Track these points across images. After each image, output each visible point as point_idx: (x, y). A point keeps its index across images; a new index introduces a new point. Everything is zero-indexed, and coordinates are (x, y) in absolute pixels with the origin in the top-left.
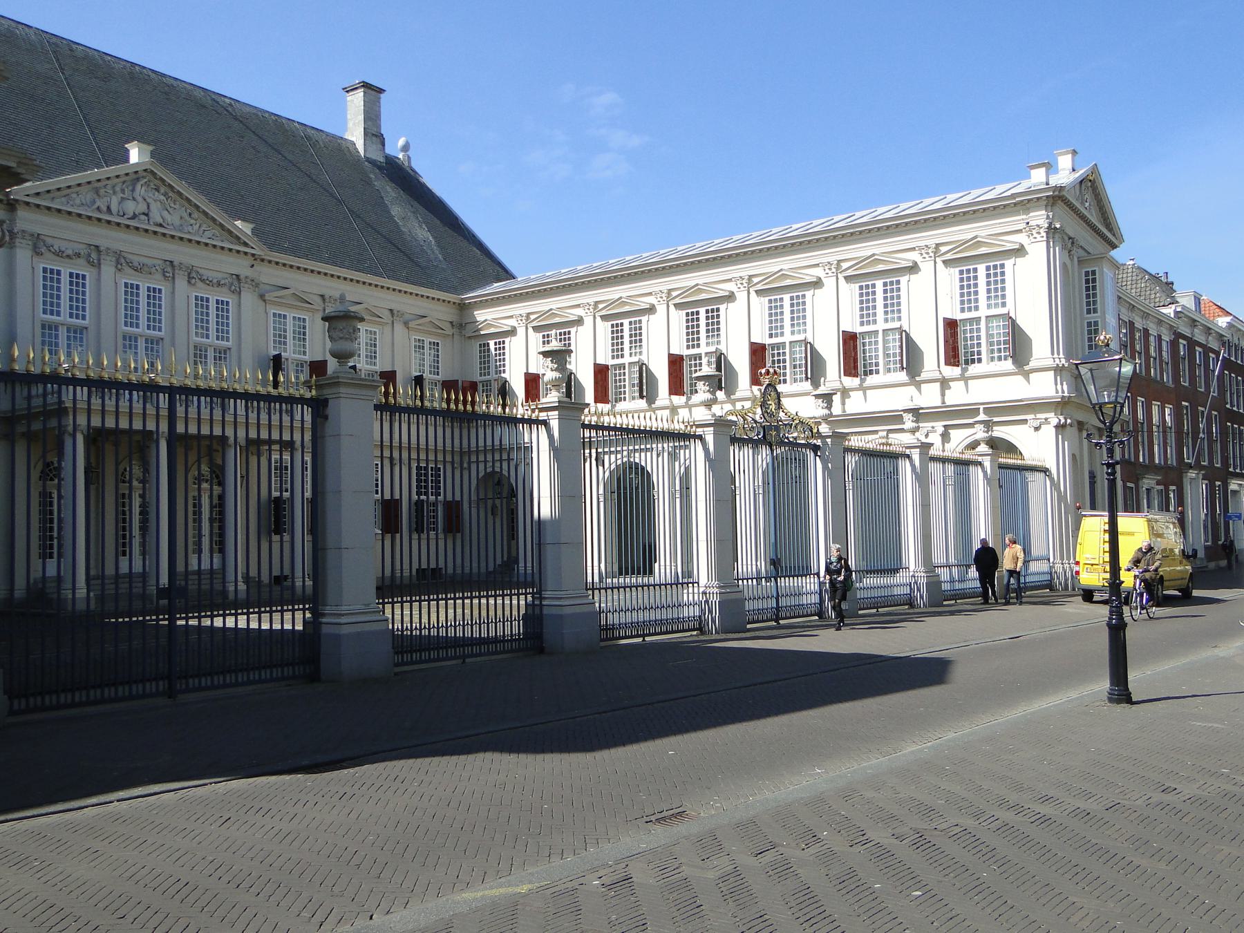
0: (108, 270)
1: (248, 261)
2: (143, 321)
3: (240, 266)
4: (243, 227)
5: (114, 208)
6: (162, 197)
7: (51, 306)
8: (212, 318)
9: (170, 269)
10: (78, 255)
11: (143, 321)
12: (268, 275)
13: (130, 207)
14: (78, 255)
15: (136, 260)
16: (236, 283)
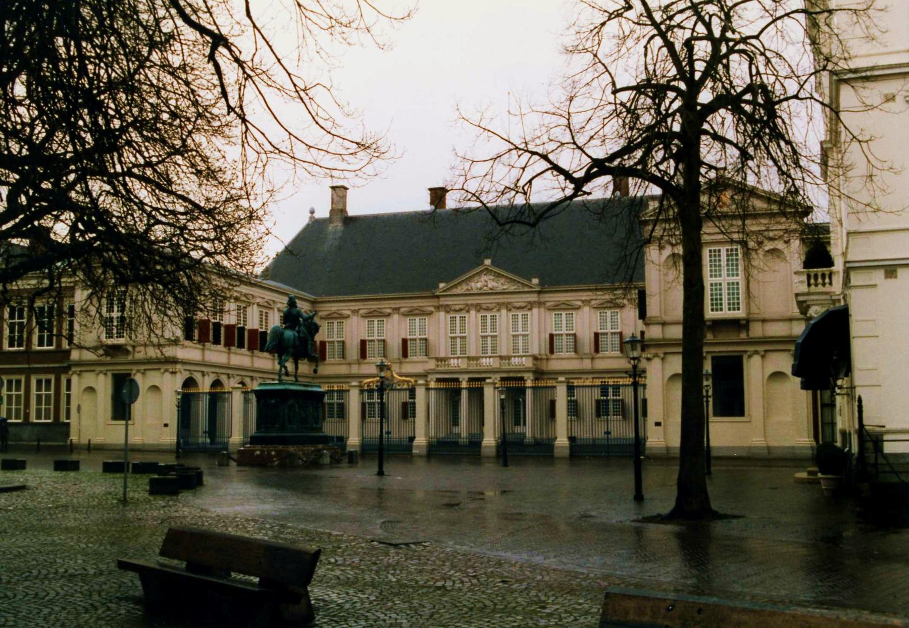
0: (473, 312)
1: (536, 295)
2: (489, 330)
3: (533, 298)
4: (535, 281)
5: (474, 288)
6: (492, 277)
7: (453, 330)
8: (520, 323)
9: (500, 306)
10: (461, 310)
12: (546, 297)
13: (479, 285)
14: (461, 310)
15: (484, 306)
16: (530, 306)
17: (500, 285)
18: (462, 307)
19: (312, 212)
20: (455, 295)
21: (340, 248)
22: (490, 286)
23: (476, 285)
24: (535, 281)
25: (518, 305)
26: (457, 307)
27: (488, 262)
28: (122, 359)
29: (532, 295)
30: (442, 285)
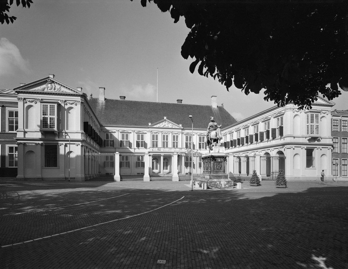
1: (181, 130)
2: (165, 140)
4: (181, 125)
11: (165, 140)
13: (162, 125)
15: (164, 132)
17: (170, 126)
18: (157, 132)
19: (91, 95)
20: (154, 128)
21: (105, 108)
22: (166, 126)
23: (161, 125)
24: (181, 125)
25: (175, 133)
26: (155, 132)
27: (165, 118)
28: (51, 137)
29: (180, 130)
30: (150, 124)
